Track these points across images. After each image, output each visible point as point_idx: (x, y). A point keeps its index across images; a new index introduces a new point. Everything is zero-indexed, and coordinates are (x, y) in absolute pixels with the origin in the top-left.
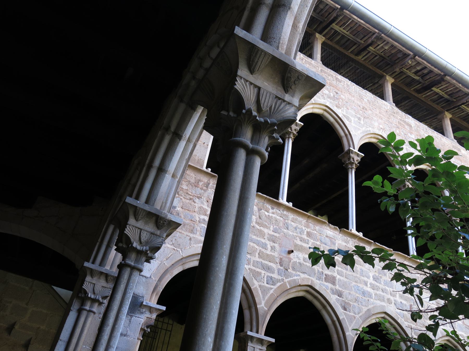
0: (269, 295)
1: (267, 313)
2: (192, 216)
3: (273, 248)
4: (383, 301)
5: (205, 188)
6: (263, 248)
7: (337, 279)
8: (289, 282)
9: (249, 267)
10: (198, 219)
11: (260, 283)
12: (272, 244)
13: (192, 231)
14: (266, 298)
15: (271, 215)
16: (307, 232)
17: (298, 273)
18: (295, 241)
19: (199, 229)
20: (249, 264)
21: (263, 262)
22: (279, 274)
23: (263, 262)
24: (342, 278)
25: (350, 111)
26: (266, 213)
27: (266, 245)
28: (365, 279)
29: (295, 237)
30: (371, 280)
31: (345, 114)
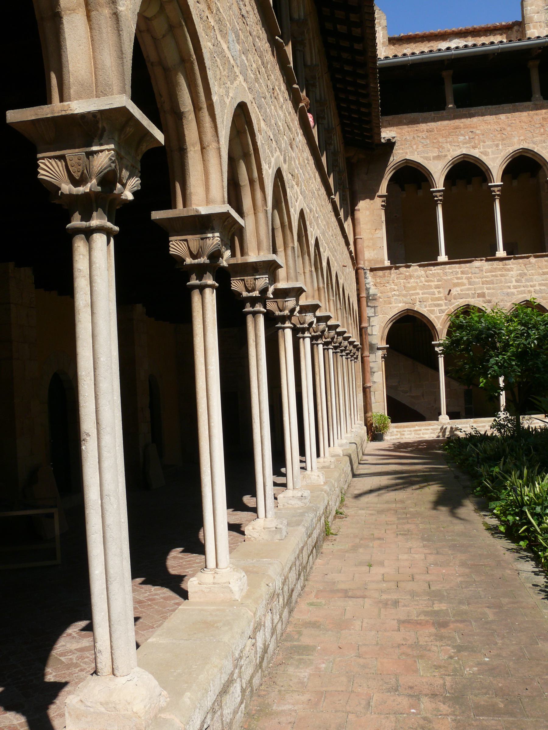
0: (441, 319)
1: (442, 330)
2: (387, 295)
3: (439, 292)
4: (525, 293)
5: (389, 275)
6: (432, 295)
7: (486, 293)
8: (453, 308)
9: (427, 309)
10: (391, 295)
11: (436, 315)
12: (438, 290)
13: (390, 303)
14: (440, 321)
15: (433, 272)
16: (461, 271)
17: (458, 300)
18: (453, 281)
19: (393, 300)
20: (426, 307)
21: (435, 302)
22: (446, 305)
23: (435, 302)
24: (490, 291)
25: (487, 143)
26: (431, 272)
27: (434, 292)
28: (509, 284)
29: (452, 279)
30: (514, 283)
31: (482, 150)
